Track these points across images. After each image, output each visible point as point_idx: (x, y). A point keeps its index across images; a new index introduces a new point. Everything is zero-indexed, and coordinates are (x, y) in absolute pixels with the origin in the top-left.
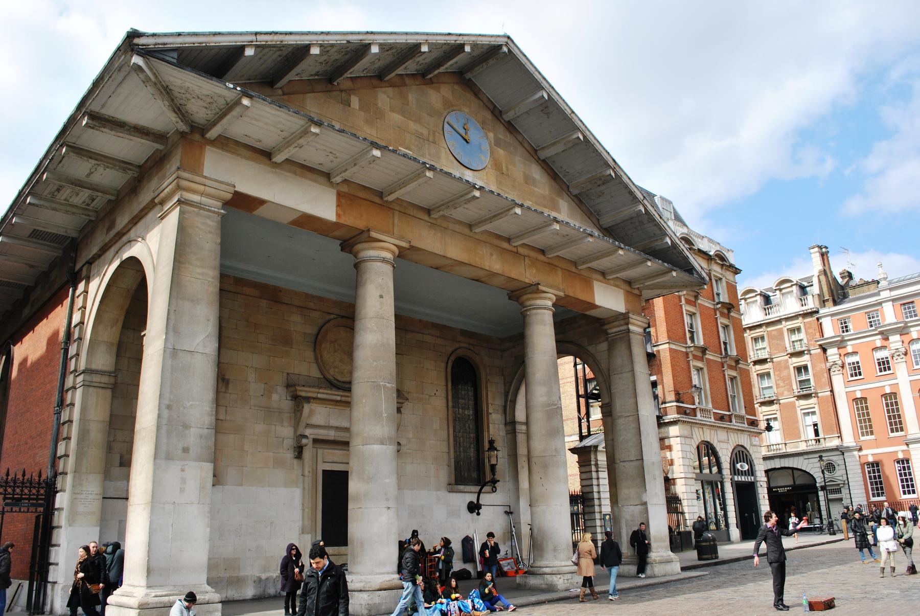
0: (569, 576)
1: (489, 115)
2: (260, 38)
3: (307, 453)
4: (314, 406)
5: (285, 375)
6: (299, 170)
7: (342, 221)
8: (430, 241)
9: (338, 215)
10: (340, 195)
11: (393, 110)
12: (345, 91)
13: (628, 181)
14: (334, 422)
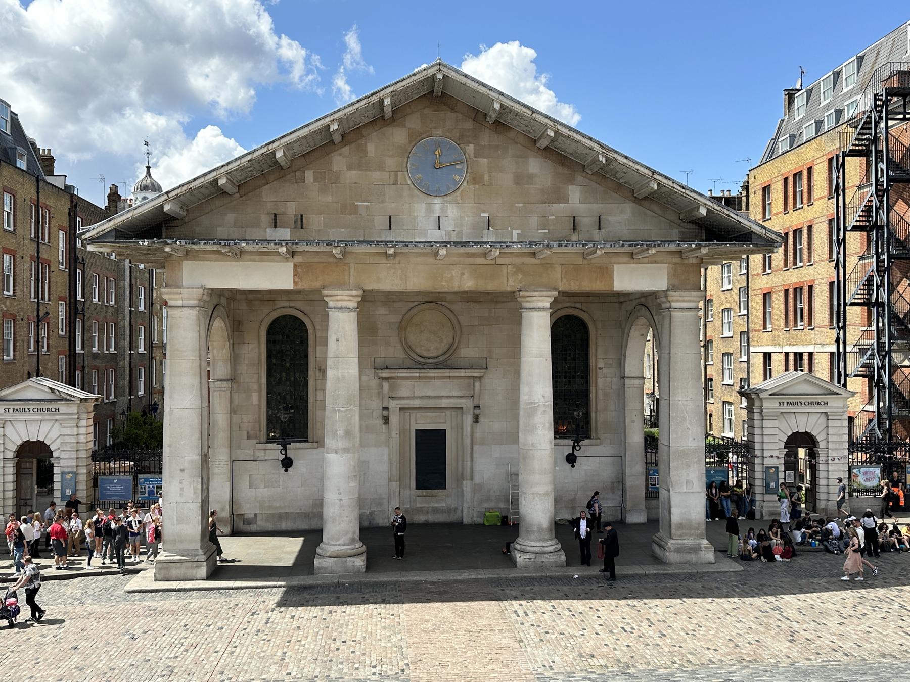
0: (533, 556)
1: (469, 125)
2: (170, 195)
3: (394, 419)
4: (399, 382)
5: (372, 359)
6: (257, 257)
7: (299, 287)
8: (387, 279)
9: (295, 283)
10: (295, 266)
11: (350, 168)
12: (299, 170)
13: (625, 161)
14: (418, 393)
